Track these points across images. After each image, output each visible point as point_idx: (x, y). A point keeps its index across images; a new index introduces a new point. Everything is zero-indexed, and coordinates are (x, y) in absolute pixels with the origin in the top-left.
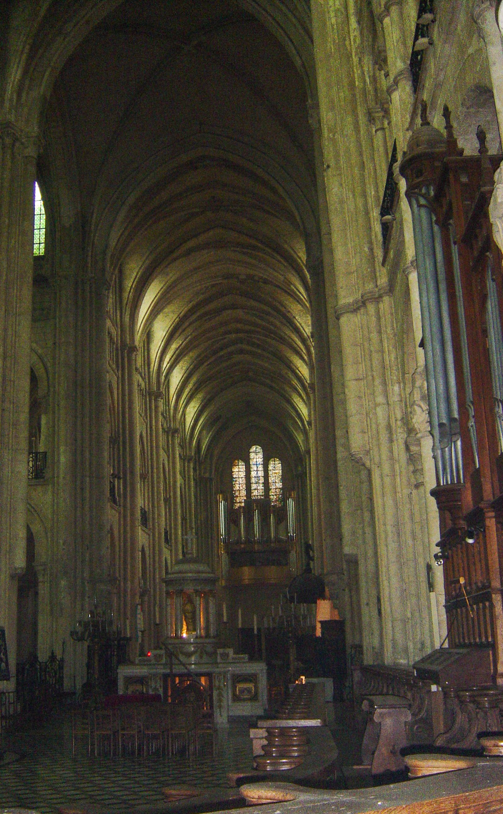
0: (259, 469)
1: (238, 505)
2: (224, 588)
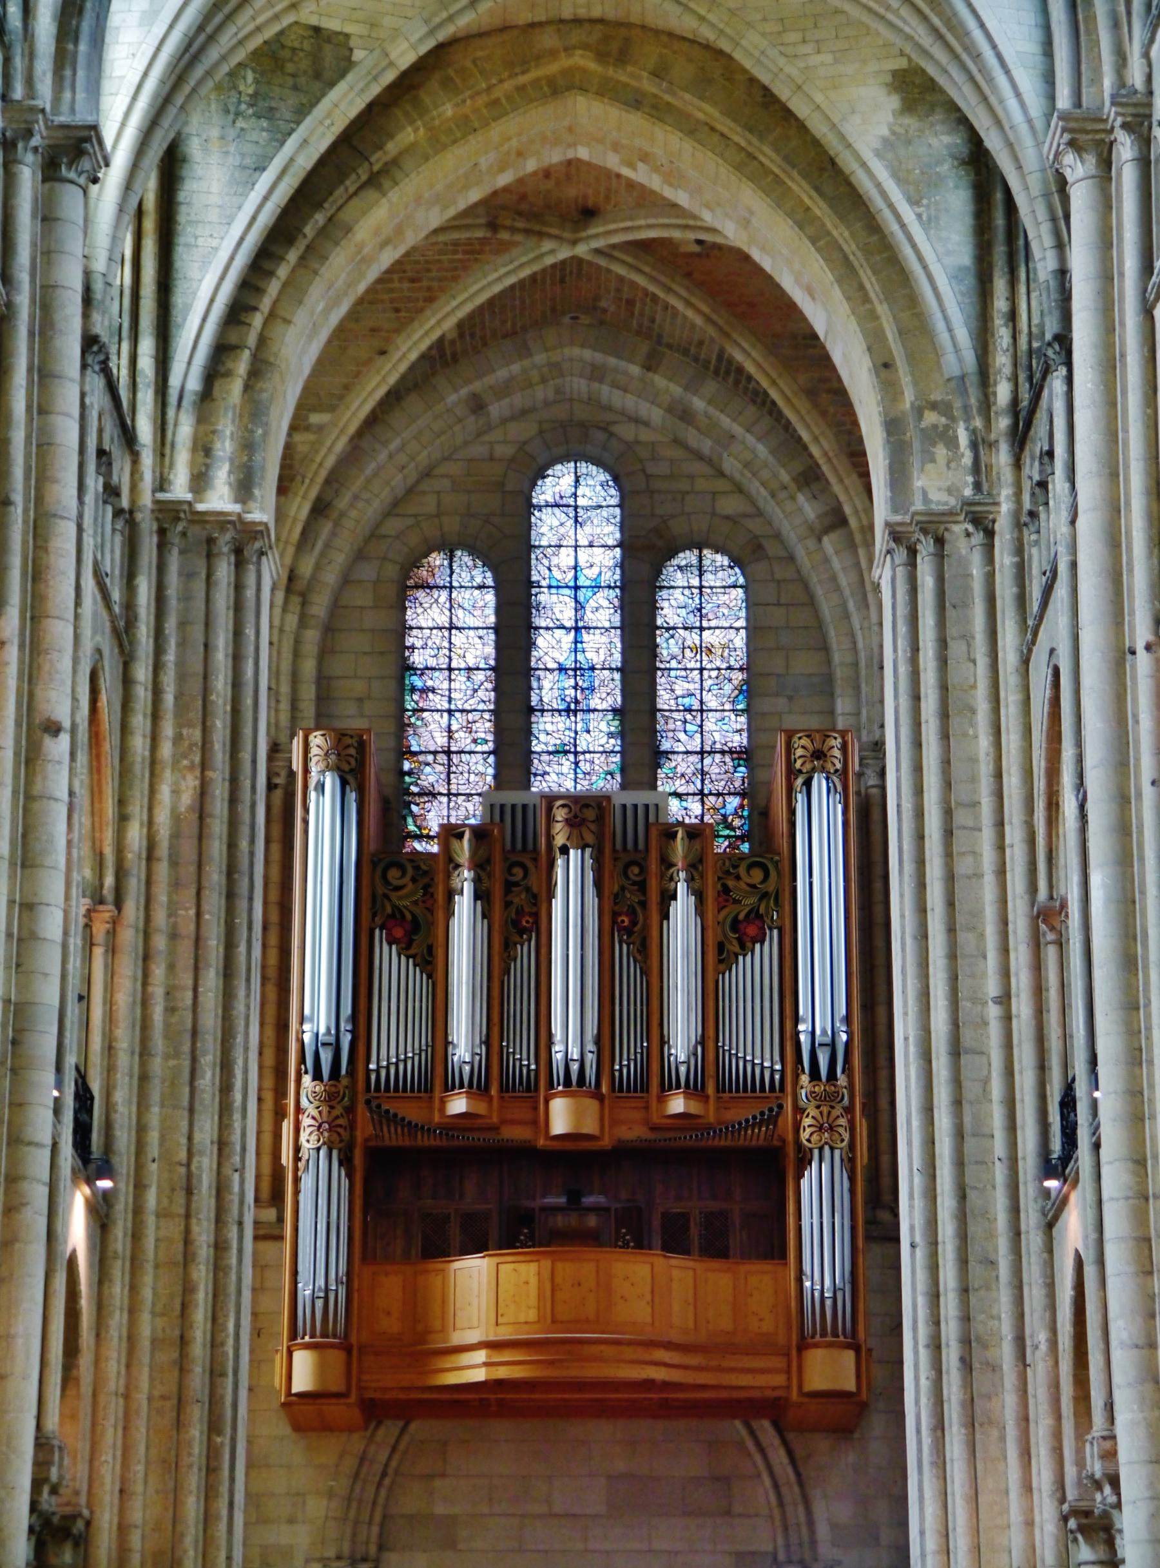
0: (590, 617)
1: (434, 817)
2: (305, 1413)
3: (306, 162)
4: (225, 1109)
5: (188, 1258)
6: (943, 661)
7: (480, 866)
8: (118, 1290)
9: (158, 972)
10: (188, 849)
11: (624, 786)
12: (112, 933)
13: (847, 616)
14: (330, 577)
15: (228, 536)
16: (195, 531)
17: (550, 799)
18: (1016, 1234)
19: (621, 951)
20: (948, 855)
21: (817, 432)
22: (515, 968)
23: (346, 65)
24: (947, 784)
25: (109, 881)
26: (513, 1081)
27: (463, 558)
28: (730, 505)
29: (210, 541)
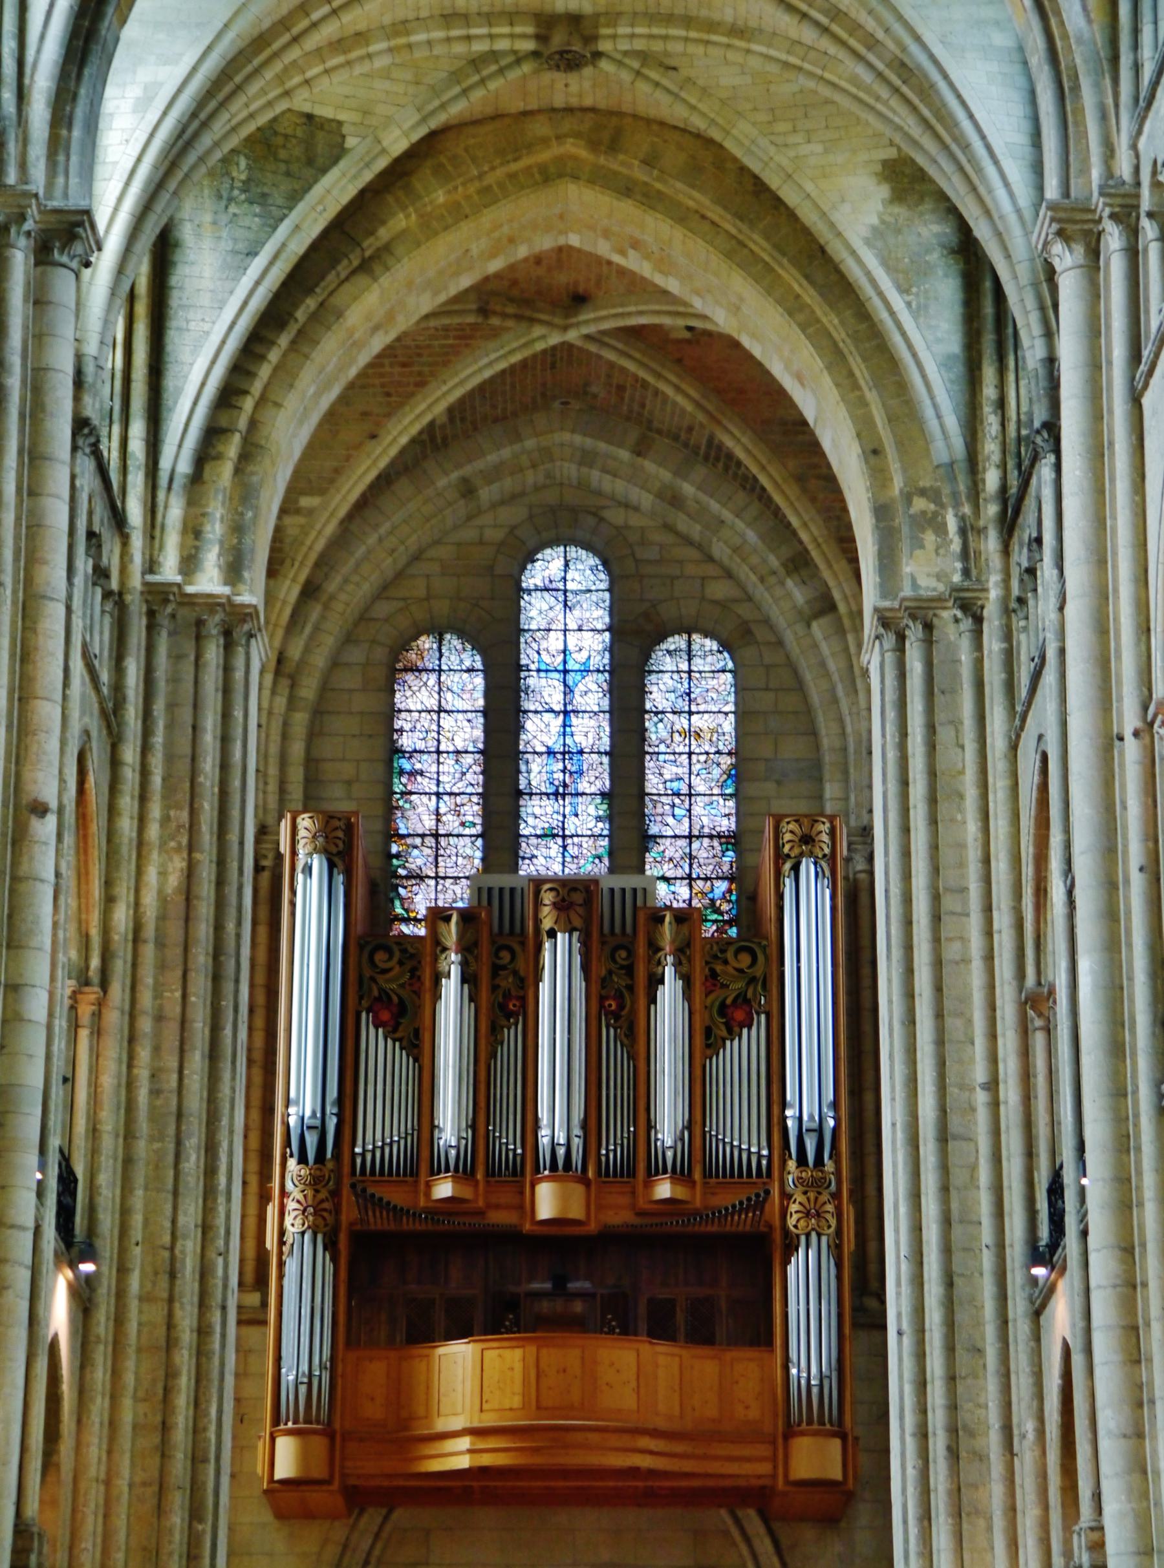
0: (579, 701)
1: (422, 900)
2: (288, 1500)
3: (298, 247)
4: (209, 1192)
5: (171, 1343)
6: (931, 747)
7: (467, 949)
8: (100, 1375)
9: (144, 1054)
10: (175, 931)
11: (612, 870)
12: (98, 1016)
13: (835, 701)
14: (320, 660)
15: (218, 618)
16: (183, 612)
17: (538, 883)
18: (1004, 1322)
19: (608, 1035)
20: (936, 940)
21: (806, 518)
22: (502, 1052)
23: (338, 152)
24: (935, 870)
25: (95, 962)
26: (500, 1166)
27: (452, 641)
28: (720, 590)
29: (200, 623)
